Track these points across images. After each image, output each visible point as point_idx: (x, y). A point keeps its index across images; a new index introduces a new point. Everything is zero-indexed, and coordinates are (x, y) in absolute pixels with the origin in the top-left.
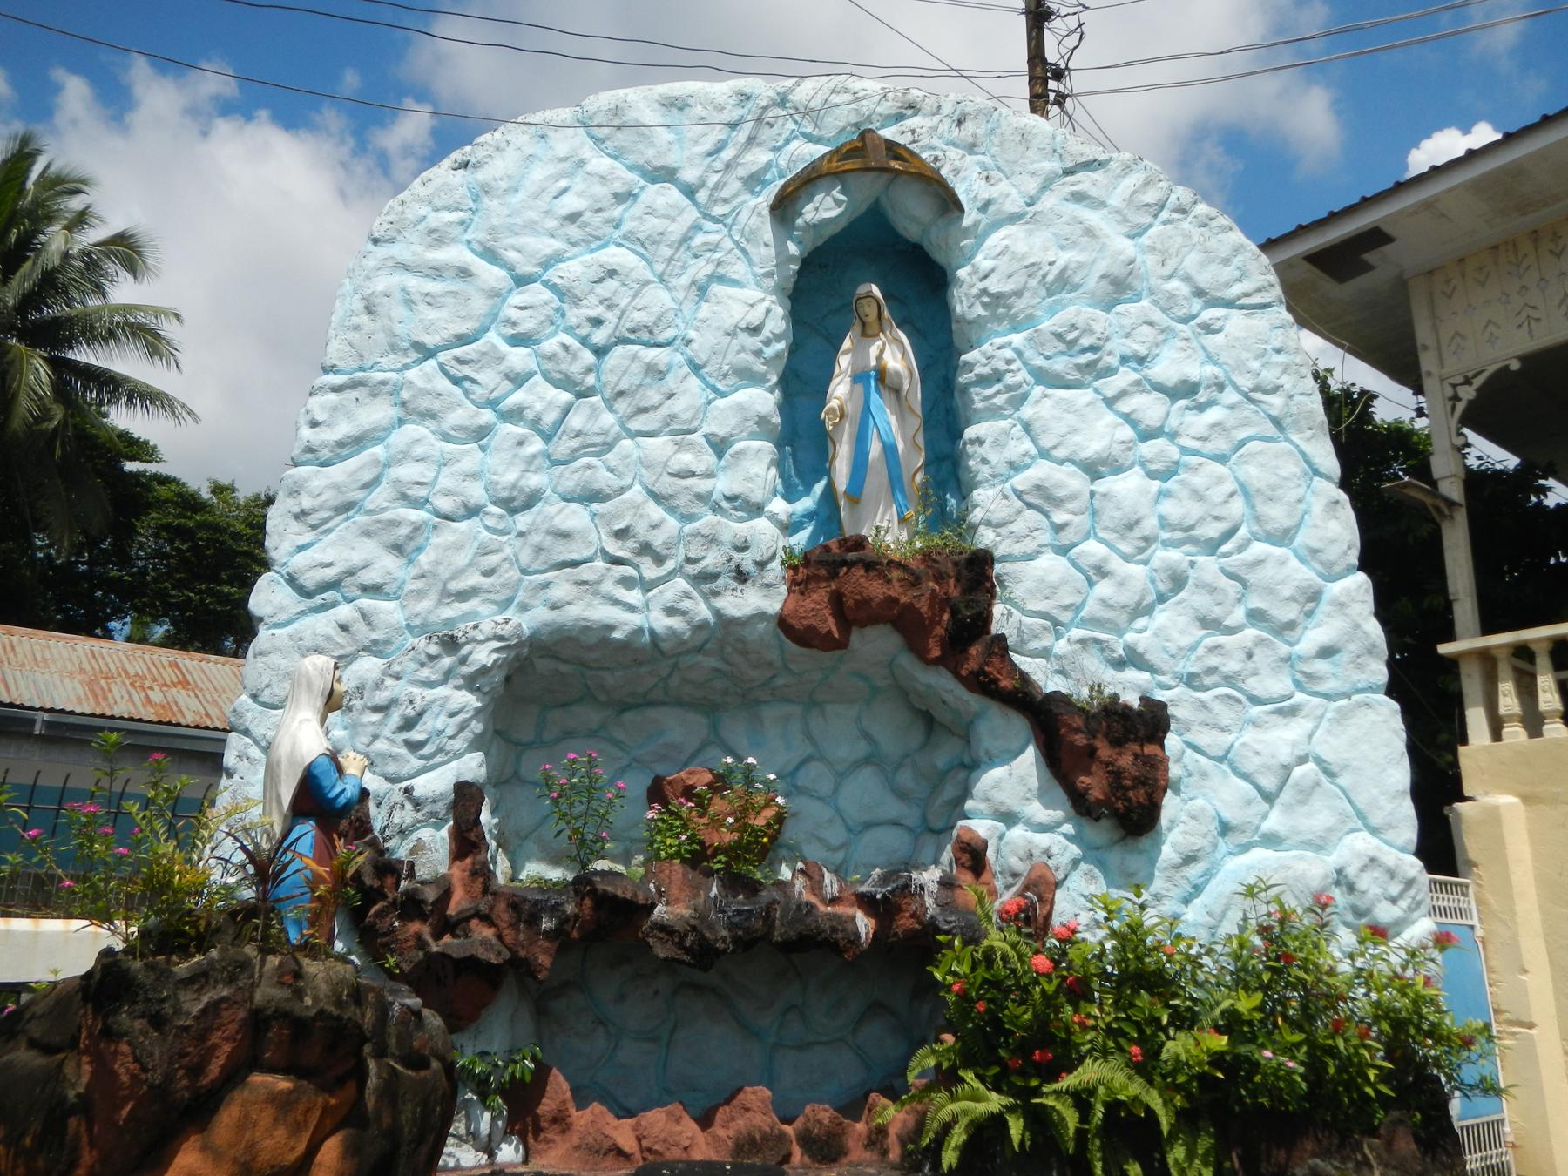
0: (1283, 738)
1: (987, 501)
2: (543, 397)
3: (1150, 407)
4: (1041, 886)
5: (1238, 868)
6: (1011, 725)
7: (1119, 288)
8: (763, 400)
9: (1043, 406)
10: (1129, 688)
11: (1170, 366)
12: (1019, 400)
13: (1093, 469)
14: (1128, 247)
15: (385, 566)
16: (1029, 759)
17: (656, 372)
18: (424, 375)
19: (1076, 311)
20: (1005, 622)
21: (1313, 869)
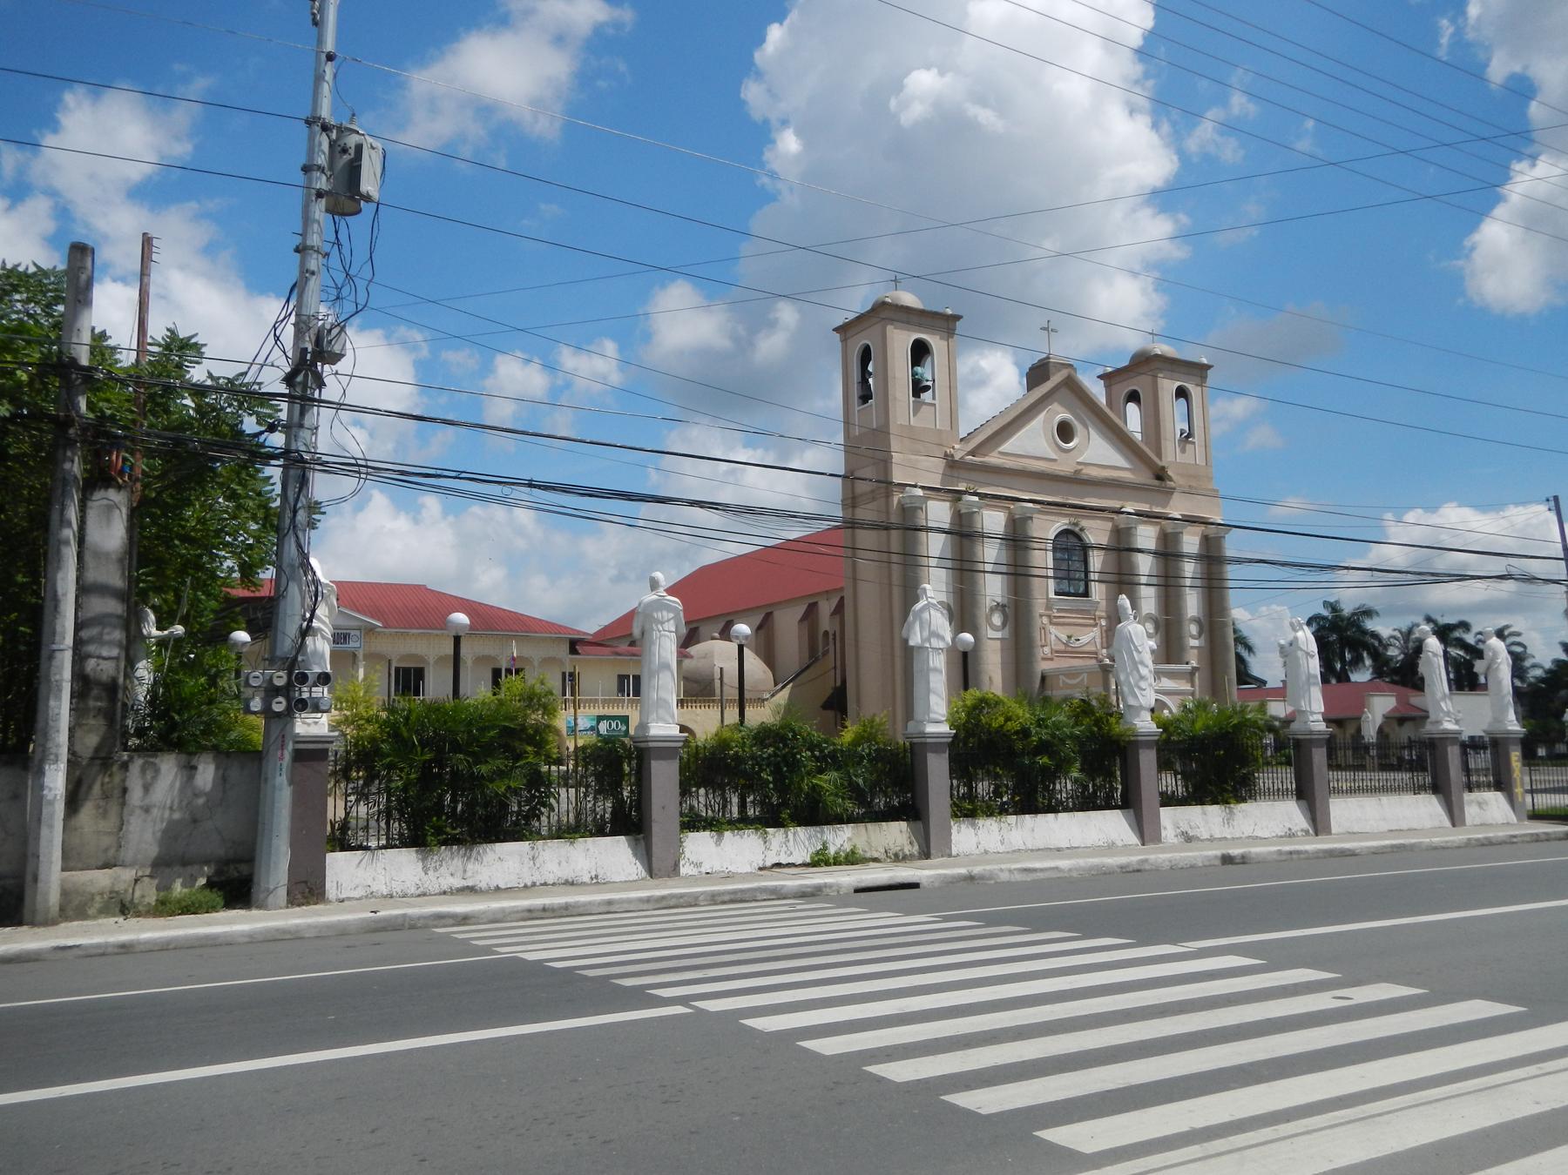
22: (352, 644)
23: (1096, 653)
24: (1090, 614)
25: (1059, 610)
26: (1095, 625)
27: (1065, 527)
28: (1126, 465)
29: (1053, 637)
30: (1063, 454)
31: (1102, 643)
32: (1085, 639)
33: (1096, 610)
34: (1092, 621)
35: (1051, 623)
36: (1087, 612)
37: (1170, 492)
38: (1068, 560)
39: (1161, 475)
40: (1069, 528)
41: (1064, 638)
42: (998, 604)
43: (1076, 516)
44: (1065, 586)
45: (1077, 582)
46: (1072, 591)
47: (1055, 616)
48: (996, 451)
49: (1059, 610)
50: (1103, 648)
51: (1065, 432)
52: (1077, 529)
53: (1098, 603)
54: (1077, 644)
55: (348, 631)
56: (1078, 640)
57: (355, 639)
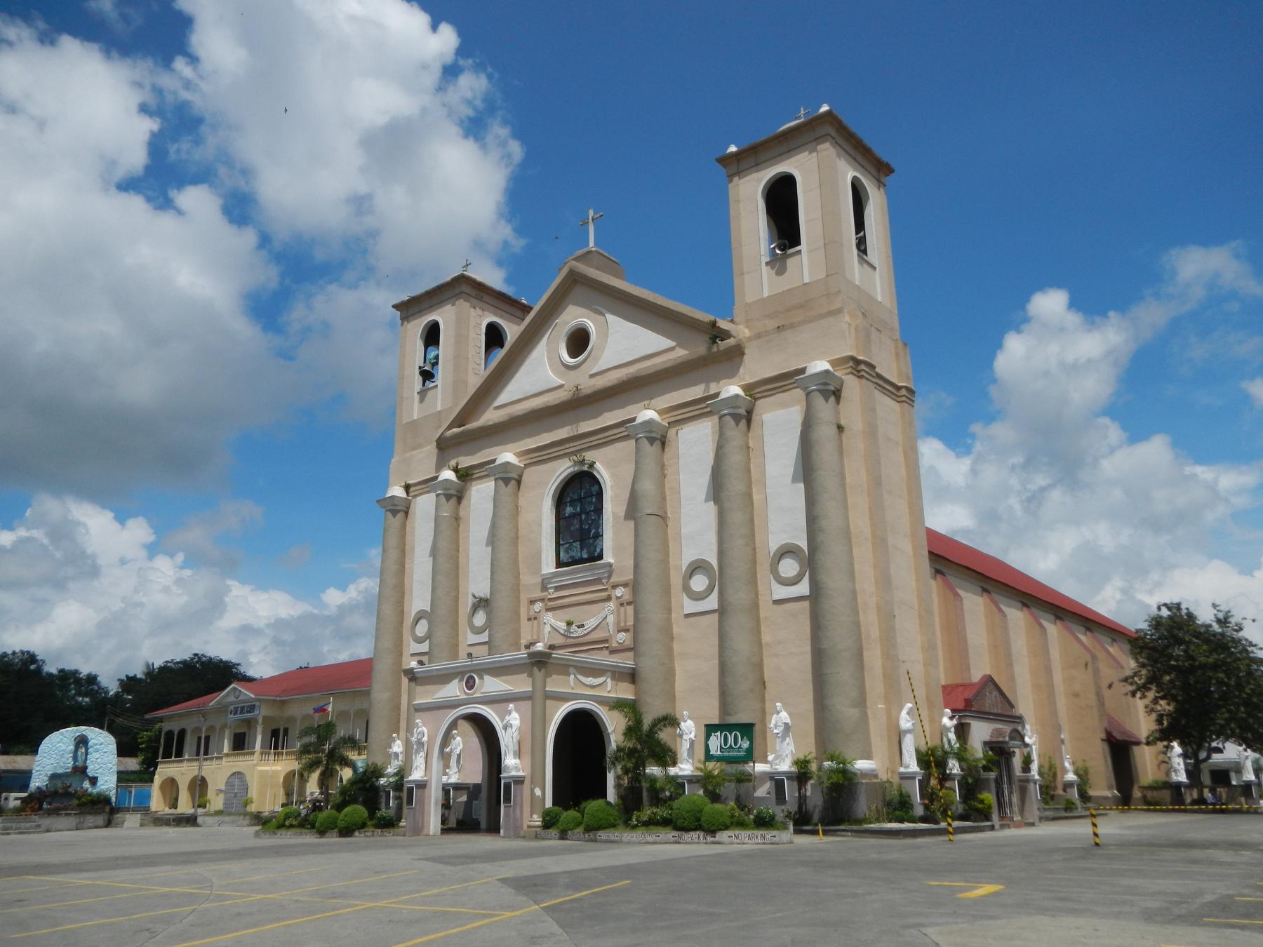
0: (107, 778)
1: (88, 762)
2: (54, 756)
3: (102, 754)
4: (87, 789)
5: (102, 787)
6: (86, 778)
7: (101, 744)
8: (71, 755)
9: (94, 754)
10: (96, 775)
11: (105, 750)
12: (91, 754)
13: (97, 759)
14: (103, 740)
15: (42, 769)
16: (88, 781)
17: (63, 754)
18: (45, 755)
19: (98, 746)
20: (87, 771)
21: (107, 787)
22: (256, 712)
23: (606, 641)
24: (603, 584)
25: (557, 589)
26: (609, 599)
27: (571, 470)
28: (665, 343)
29: (547, 629)
30: (572, 373)
31: (618, 623)
32: (591, 623)
33: (609, 577)
34: (605, 594)
35: (548, 610)
36: (598, 581)
37: (737, 352)
38: (580, 514)
39: (716, 334)
40: (576, 469)
41: (562, 626)
42: (481, 599)
43: (574, 453)
44: (576, 552)
45: (591, 541)
46: (585, 556)
47: (550, 600)
48: (492, 408)
49: (557, 589)
50: (619, 631)
51: (579, 341)
52: (586, 468)
53: (610, 565)
54: (580, 632)
55: (254, 703)
56: (583, 626)
57: (257, 708)
